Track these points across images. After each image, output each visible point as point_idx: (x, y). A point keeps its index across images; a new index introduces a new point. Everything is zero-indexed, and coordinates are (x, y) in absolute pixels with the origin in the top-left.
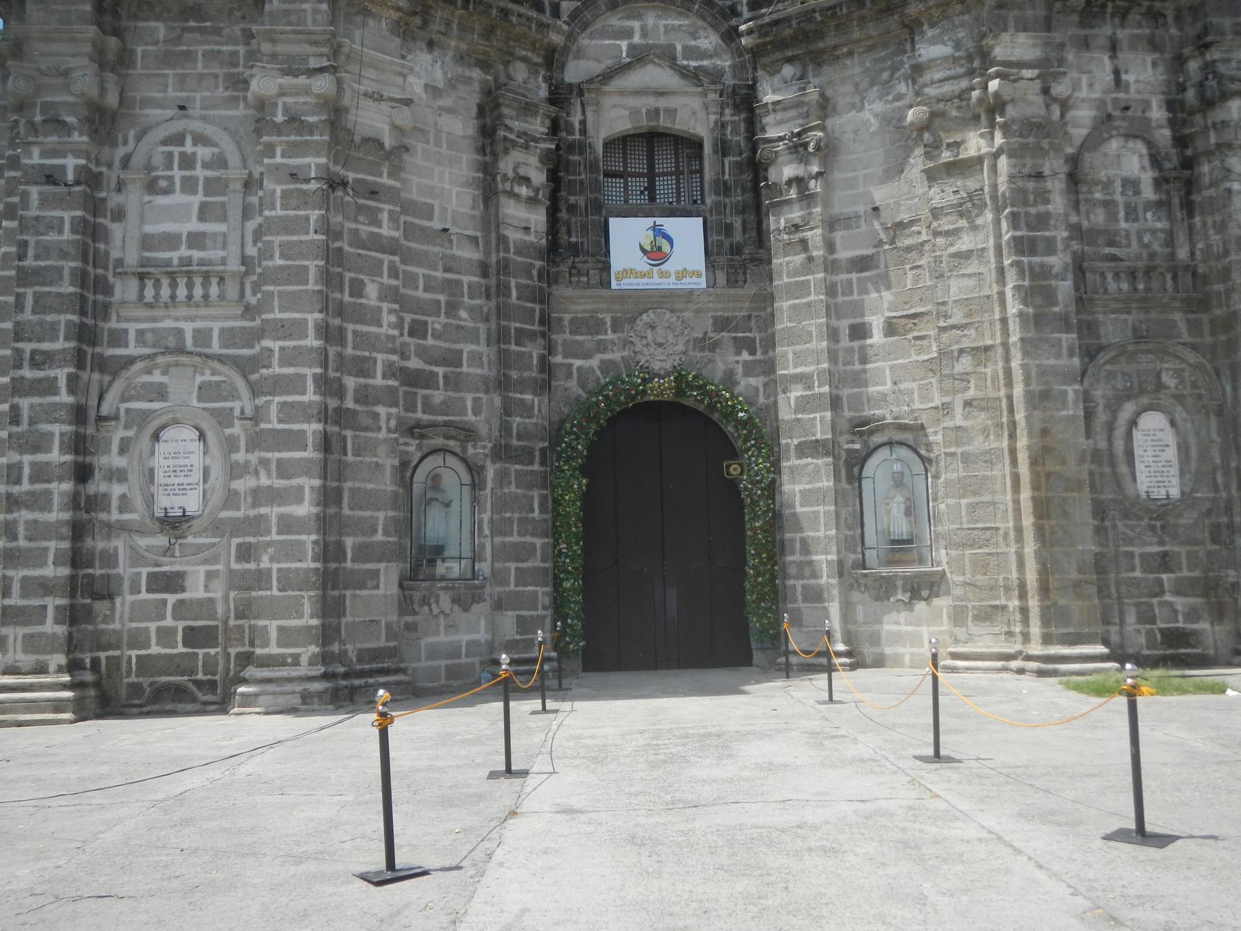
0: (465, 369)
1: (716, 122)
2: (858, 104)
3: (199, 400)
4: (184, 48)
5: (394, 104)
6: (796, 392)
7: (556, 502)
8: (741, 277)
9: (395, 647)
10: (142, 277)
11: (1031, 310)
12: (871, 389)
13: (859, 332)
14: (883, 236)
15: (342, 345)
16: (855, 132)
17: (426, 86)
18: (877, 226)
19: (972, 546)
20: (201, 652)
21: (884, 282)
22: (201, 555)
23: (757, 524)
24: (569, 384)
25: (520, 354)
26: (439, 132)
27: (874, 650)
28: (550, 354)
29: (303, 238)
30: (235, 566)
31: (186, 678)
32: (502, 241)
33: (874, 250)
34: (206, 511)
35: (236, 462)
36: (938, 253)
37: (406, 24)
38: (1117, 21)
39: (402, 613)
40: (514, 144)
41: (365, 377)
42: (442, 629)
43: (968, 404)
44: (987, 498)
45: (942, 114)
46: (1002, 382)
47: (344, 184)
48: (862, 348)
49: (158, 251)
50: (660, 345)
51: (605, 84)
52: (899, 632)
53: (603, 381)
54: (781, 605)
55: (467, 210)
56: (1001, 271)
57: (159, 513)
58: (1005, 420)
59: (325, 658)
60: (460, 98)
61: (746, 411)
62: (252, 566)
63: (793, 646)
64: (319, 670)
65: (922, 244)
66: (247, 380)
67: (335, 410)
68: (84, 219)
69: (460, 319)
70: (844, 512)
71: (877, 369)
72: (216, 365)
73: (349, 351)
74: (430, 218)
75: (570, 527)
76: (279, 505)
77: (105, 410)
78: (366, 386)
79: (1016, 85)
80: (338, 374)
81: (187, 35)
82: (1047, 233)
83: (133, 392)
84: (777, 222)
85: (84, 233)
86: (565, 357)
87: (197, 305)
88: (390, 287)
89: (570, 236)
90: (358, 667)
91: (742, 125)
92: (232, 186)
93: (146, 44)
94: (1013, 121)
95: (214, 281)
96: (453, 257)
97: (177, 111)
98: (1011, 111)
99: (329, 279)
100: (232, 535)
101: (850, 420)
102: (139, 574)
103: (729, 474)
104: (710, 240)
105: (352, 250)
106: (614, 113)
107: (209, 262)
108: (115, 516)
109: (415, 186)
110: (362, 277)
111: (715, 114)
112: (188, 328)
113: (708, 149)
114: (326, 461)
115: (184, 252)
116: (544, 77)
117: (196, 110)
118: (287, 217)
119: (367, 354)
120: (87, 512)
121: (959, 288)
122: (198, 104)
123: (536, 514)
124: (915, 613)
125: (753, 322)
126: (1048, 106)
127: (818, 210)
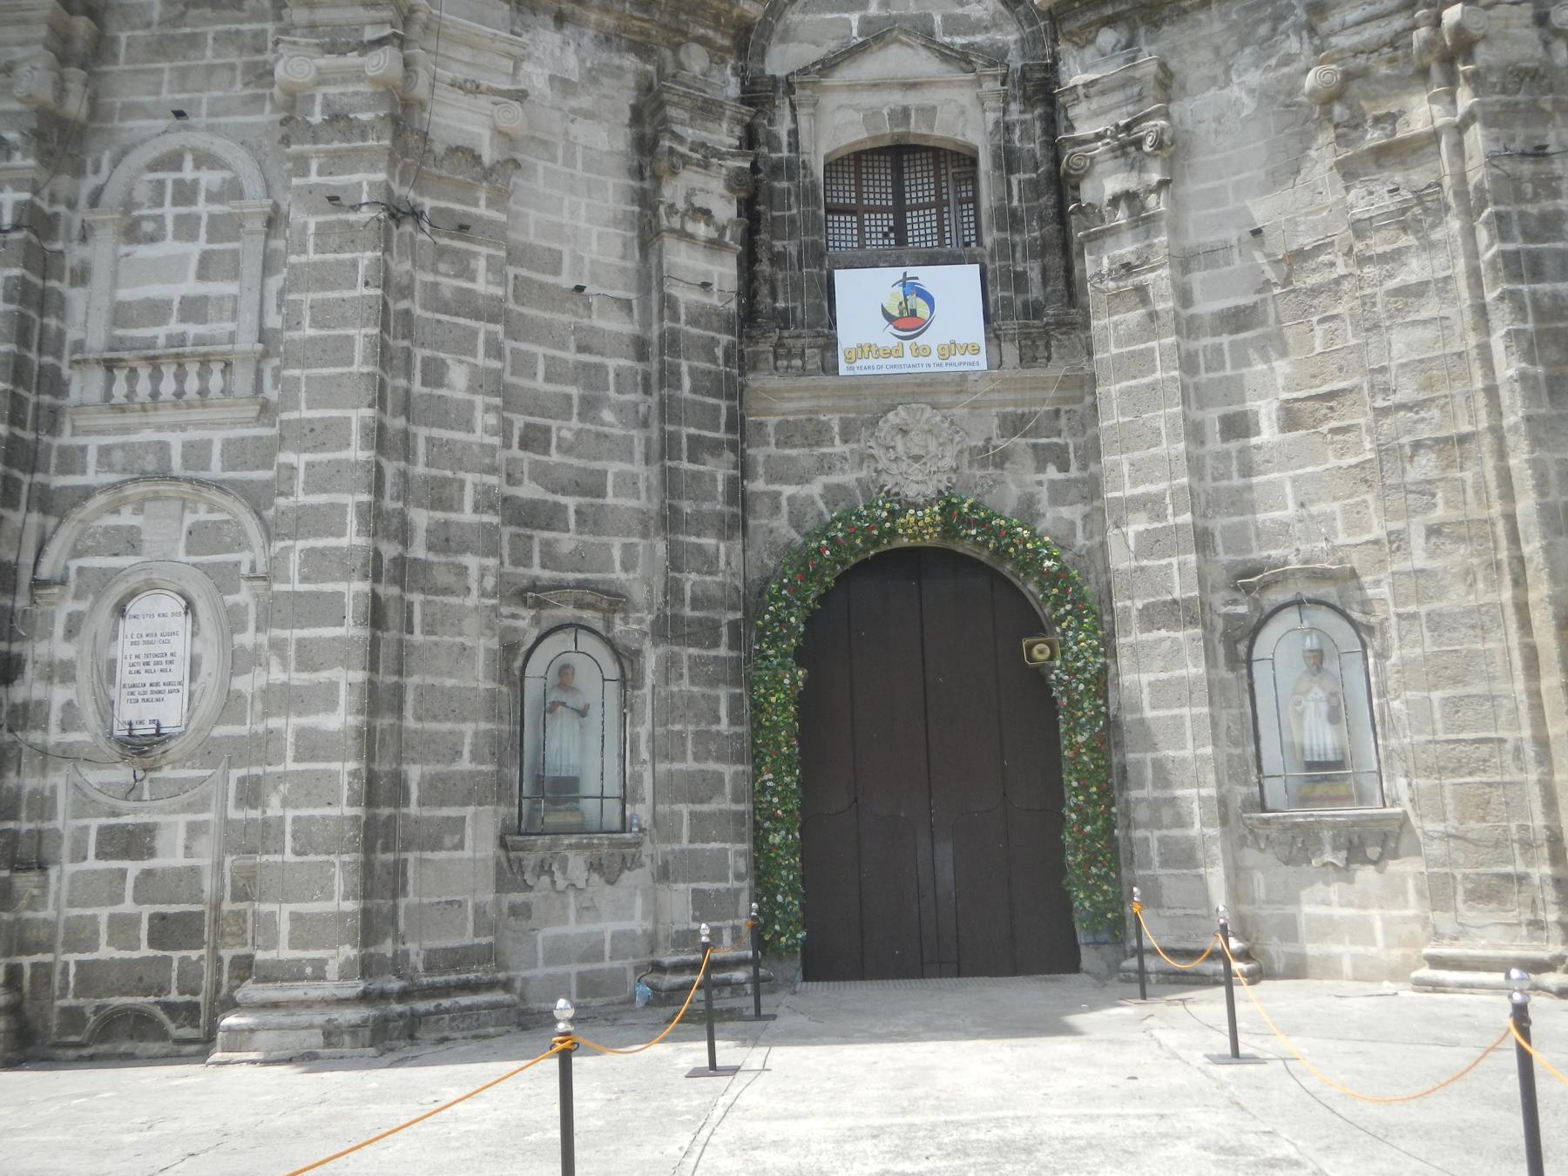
0: (610, 500)
1: (997, 123)
2: (1222, 78)
3: (188, 553)
4: (188, 30)
5: (498, 99)
6: (1137, 525)
7: (756, 707)
8: (1042, 352)
9: (490, 945)
10: (110, 365)
11: (1540, 370)
12: (1260, 517)
13: (1238, 426)
14: (1271, 274)
15: (407, 459)
16: (1218, 120)
17: (552, 78)
18: (1259, 258)
19: (1455, 771)
20: (176, 955)
21: (1278, 345)
22: (183, 797)
23: (1080, 739)
24: (775, 524)
25: (696, 476)
26: (570, 145)
27: (1289, 948)
28: (743, 477)
29: (347, 294)
30: (234, 814)
31: (151, 999)
32: (668, 303)
33: (1257, 298)
34: (192, 727)
35: (242, 647)
36: (1368, 291)
39: (501, 886)
40: (686, 161)
41: (444, 509)
42: (572, 913)
43: (1433, 531)
44: (1479, 688)
45: (1363, 74)
46: (1494, 492)
47: (416, 214)
48: (1243, 452)
49: (136, 326)
50: (917, 458)
52: (1330, 918)
53: (828, 518)
54: (1124, 871)
55: (614, 260)
56: (1481, 311)
57: (120, 731)
58: (1503, 555)
59: (367, 967)
60: (605, 96)
61: (1056, 559)
62: (255, 814)
63: (1150, 940)
64: (357, 986)
65: (1338, 282)
66: (261, 518)
67: (394, 560)
68: (23, 280)
70: (1225, 717)
71: (1270, 482)
72: (214, 495)
73: (420, 469)
74: (556, 271)
75: (779, 748)
76: (299, 714)
77: (45, 571)
78: (446, 524)
79: (1491, 13)
80: (400, 505)
83: (90, 543)
84: (1096, 264)
85: (22, 302)
86: (771, 479)
87: (190, 406)
88: (487, 371)
89: (775, 299)
90: (425, 980)
91: (1038, 128)
92: (248, 226)
93: (133, 28)
94: (1489, 69)
95: (217, 368)
97: (173, 120)
98: (1482, 54)
99: (383, 354)
100: (231, 765)
101: (1229, 567)
102: (86, 828)
103: (1031, 659)
104: (991, 298)
105: (429, 315)
107: (212, 340)
108: (54, 736)
110: (442, 355)
111: (994, 110)
112: (175, 440)
113: (985, 164)
114: (374, 643)
115: (174, 326)
116: (734, 68)
117: (200, 119)
118: (323, 263)
119: (449, 474)
120: (11, 730)
121: (1408, 344)
122: (204, 110)
123: (724, 726)
124: (1357, 886)
125: (1063, 421)
127: (1162, 239)
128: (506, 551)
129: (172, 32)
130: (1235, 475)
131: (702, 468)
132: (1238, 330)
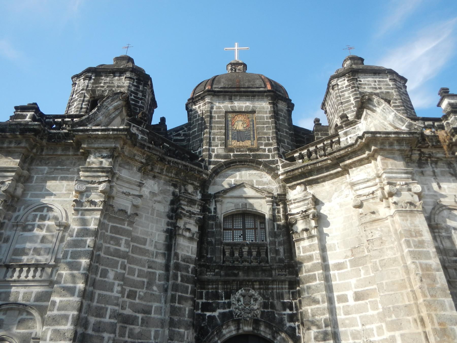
4: (53, 176)
17: (150, 192)
25: (180, 309)
26: (153, 210)
29: (82, 249)
37: (144, 169)
38: (433, 166)
40: (185, 215)
51: (225, 194)
67: (81, 334)
69: (153, 291)
73: (95, 304)
74: (145, 244)
78: (100, 322)
80: (86, 315)
81: (56, 171)
82: (425, 249)
88: (120, 273)
89: (207, 255)
91: (281, 210)
96: (153, 261)
106: (229, 205)
109: (139, 232)
110: (107, 268)
118: (77, 240)
119: (103, 305)
126: (412, 196)
128: (117, 331)
129: (49, 176)
130: (342, 314)
131: (182, 306)
132: (339, 269)
